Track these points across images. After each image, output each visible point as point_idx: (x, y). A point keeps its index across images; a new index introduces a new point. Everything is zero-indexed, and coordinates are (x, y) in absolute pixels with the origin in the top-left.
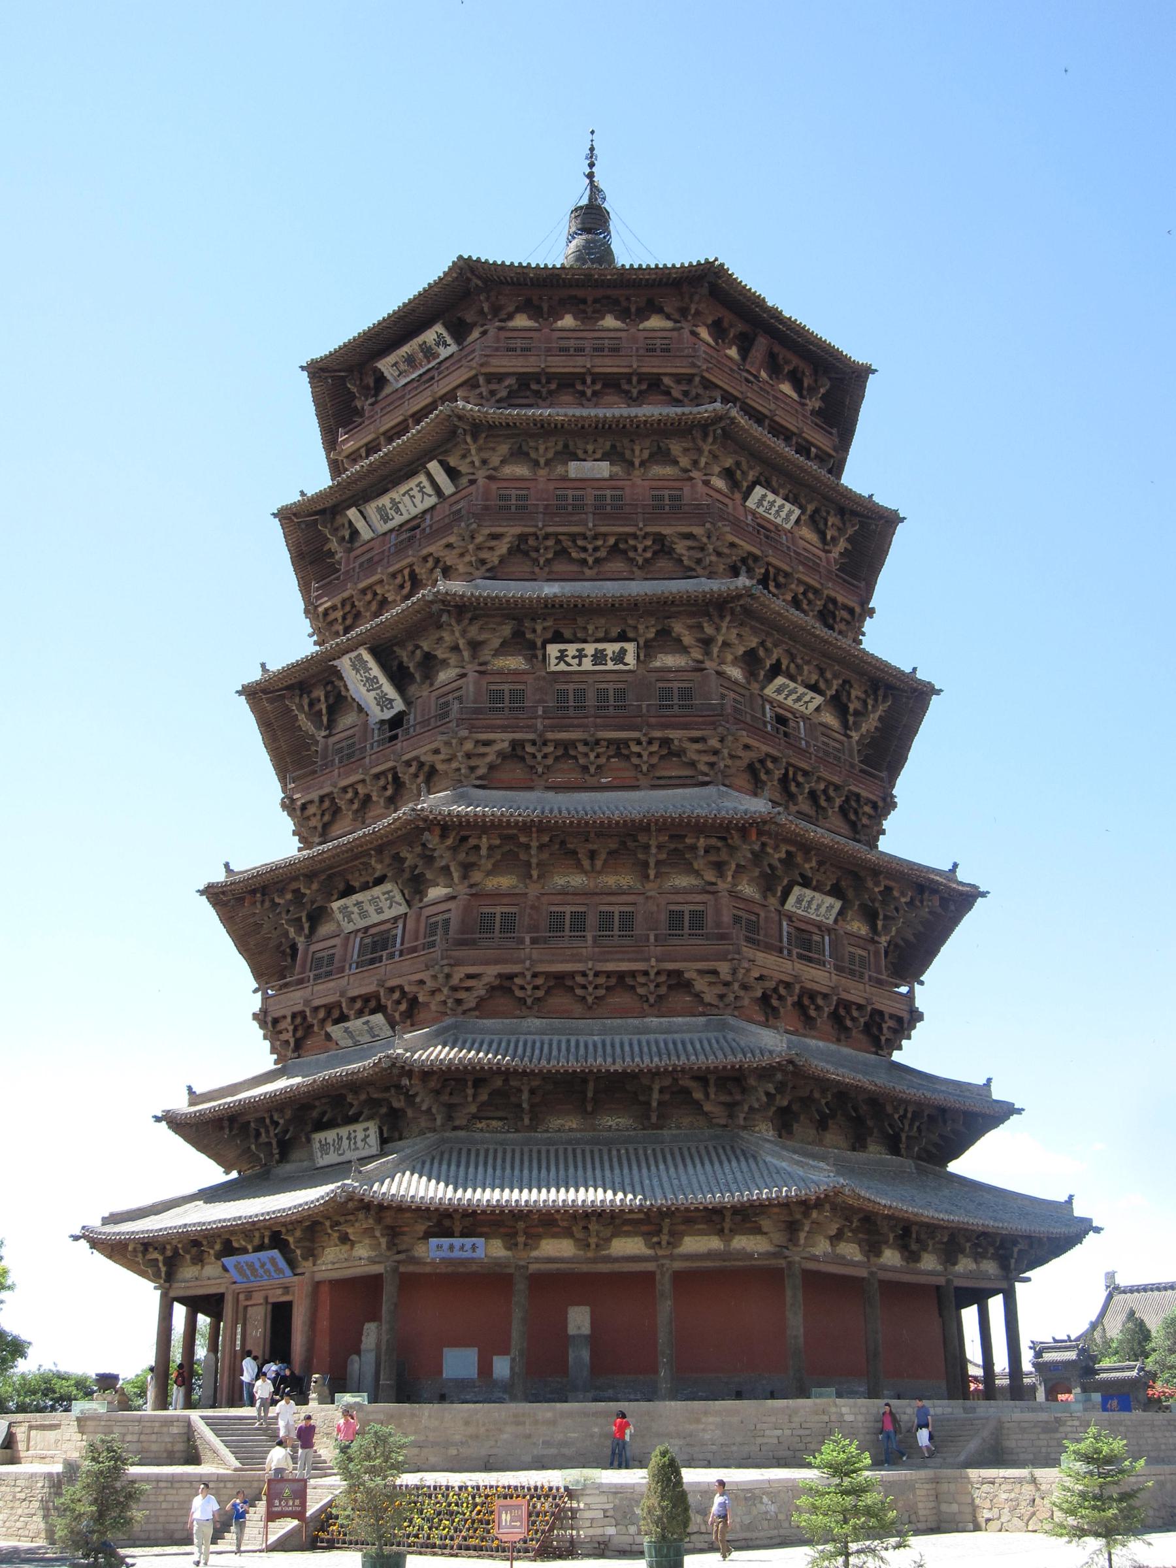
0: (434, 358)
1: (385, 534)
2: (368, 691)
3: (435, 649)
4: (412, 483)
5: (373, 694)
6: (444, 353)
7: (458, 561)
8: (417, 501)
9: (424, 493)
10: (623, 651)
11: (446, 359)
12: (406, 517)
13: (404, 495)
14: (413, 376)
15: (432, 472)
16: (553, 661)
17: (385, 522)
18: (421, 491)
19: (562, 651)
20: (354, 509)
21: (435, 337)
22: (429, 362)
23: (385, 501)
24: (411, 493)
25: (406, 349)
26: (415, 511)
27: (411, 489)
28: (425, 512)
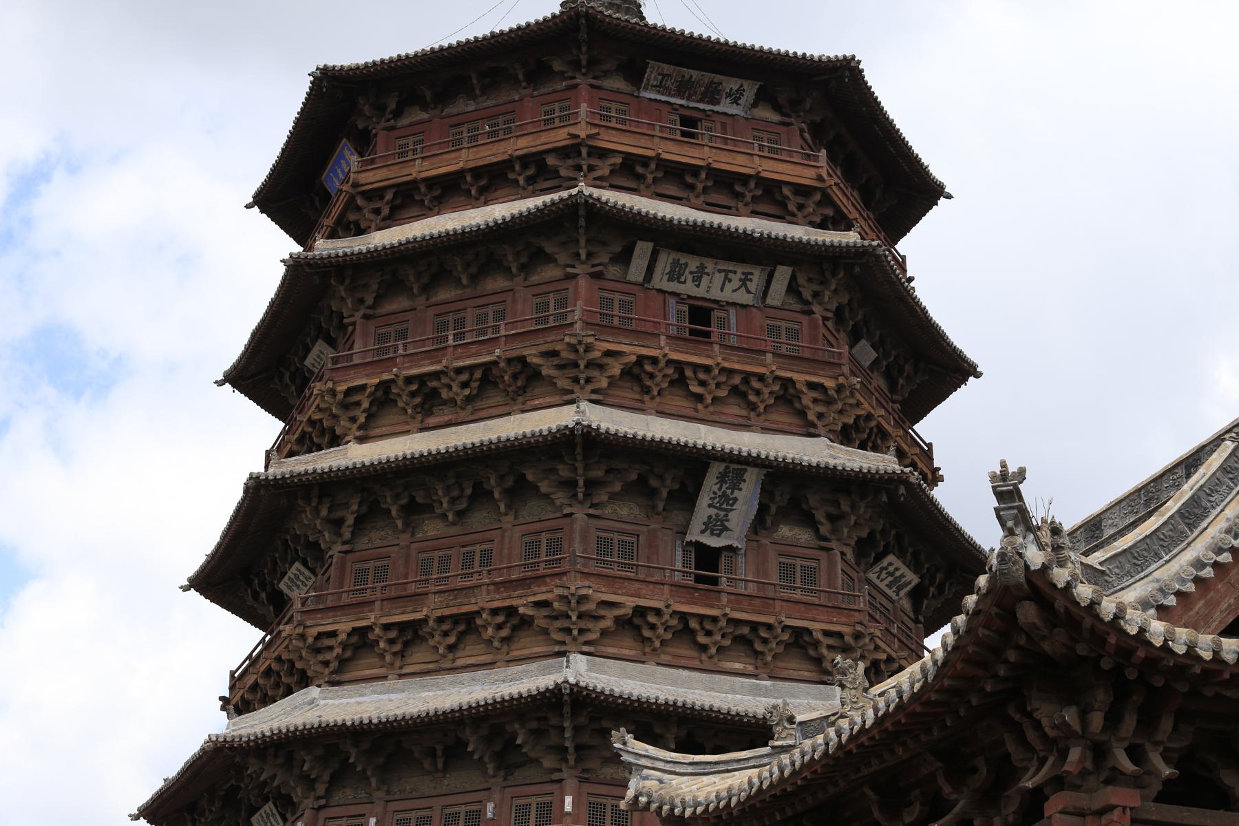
0: (708, 103)
1: (660, 291)
2: (710, 506)
3: (816, 509)
4: (740, 269)
5: (713, 511)
6: (725, 106)
7: (811, 405)
8: (729, 287)
9: (744, 284)
10: (910, 583)
11: (725, 114)
12: (700, 292)
13: (720, 271)
14: (672, 100)
15: (777, 275)
16: (877, 569)
17: (670, 279)
18: (744, 282)
19: (890, 564)
20: (651, 245)
21: (735, 88)
22: (699, 101)
23: (693, 263)
24: (731, 276)
25: (695, 74)
26: (715, 294)
27: (735, 272)
28: (734, 304)
